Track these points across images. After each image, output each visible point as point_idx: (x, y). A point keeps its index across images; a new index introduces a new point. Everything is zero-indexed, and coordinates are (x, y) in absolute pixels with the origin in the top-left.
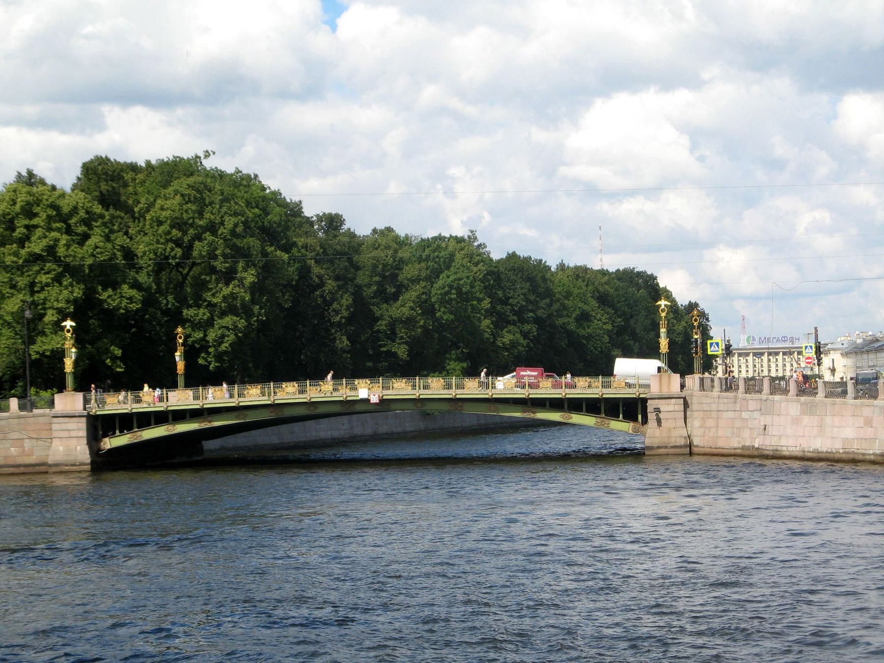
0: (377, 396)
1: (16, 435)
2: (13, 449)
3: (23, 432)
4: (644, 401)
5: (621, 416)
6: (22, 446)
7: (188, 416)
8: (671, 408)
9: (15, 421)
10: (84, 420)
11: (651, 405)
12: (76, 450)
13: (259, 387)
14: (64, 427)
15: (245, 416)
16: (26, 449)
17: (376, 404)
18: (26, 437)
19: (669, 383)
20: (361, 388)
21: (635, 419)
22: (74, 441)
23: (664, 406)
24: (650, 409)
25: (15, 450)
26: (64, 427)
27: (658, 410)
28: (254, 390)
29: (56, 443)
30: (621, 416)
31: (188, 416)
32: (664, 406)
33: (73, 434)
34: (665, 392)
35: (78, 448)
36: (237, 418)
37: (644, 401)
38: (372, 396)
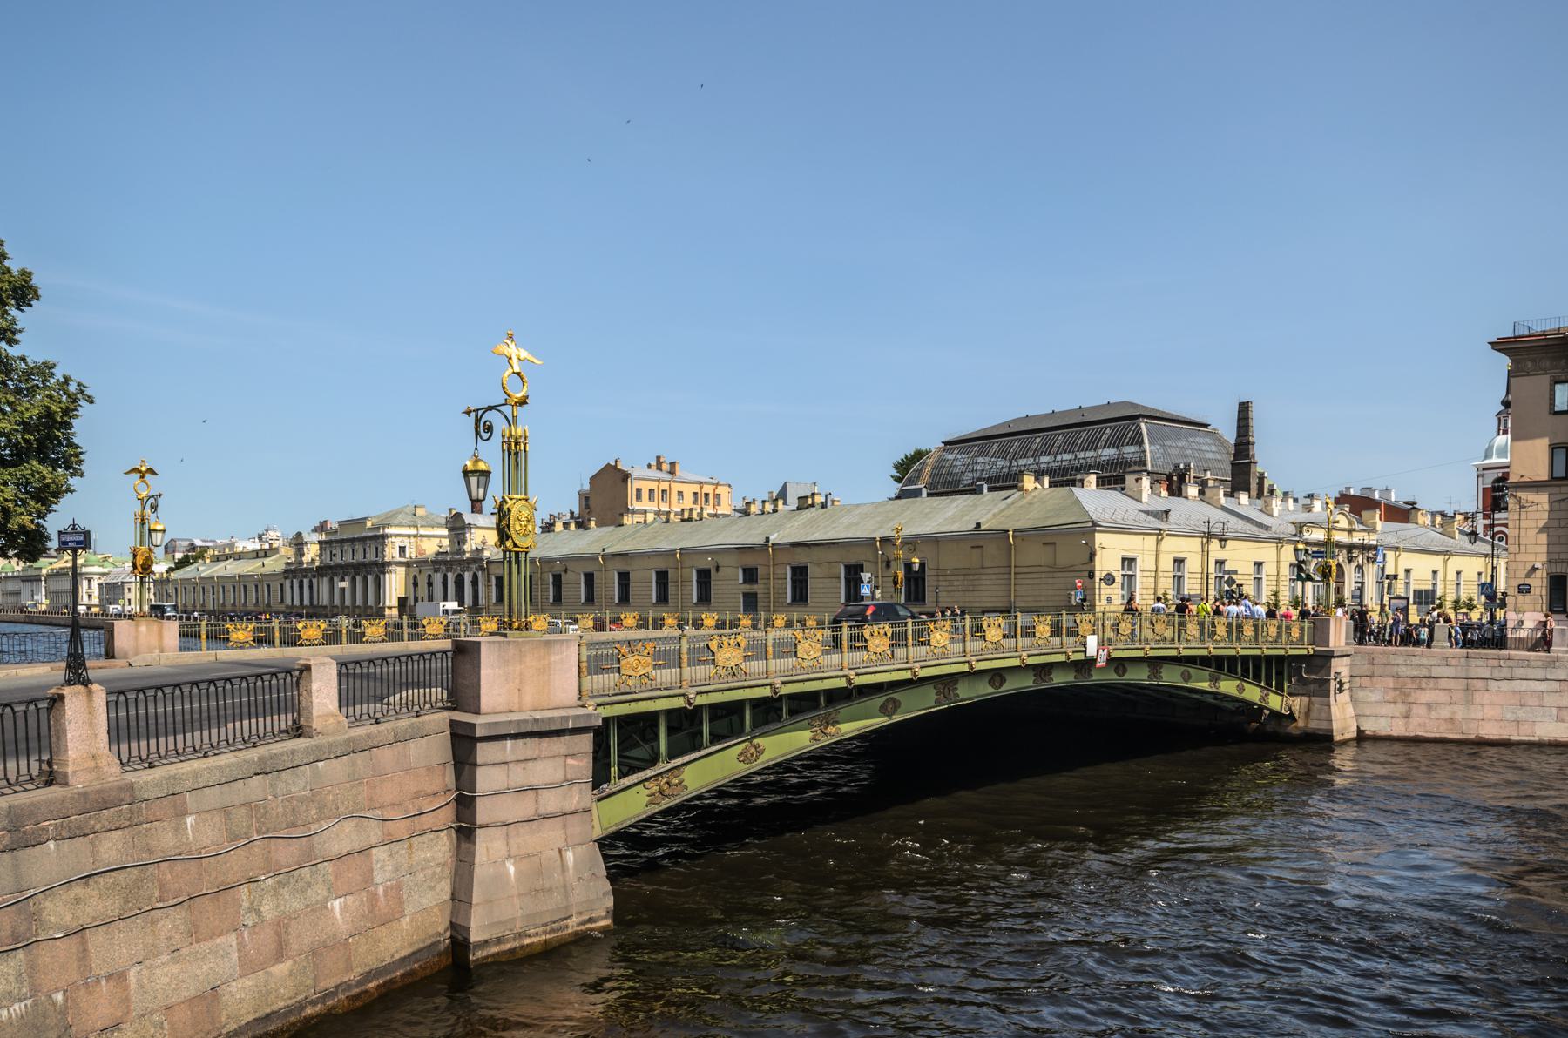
2: (336, 904)
22: (552, 834)
25: (344, 909)
26: (519, 776)
29: (487, 846)
33: (551, 802)
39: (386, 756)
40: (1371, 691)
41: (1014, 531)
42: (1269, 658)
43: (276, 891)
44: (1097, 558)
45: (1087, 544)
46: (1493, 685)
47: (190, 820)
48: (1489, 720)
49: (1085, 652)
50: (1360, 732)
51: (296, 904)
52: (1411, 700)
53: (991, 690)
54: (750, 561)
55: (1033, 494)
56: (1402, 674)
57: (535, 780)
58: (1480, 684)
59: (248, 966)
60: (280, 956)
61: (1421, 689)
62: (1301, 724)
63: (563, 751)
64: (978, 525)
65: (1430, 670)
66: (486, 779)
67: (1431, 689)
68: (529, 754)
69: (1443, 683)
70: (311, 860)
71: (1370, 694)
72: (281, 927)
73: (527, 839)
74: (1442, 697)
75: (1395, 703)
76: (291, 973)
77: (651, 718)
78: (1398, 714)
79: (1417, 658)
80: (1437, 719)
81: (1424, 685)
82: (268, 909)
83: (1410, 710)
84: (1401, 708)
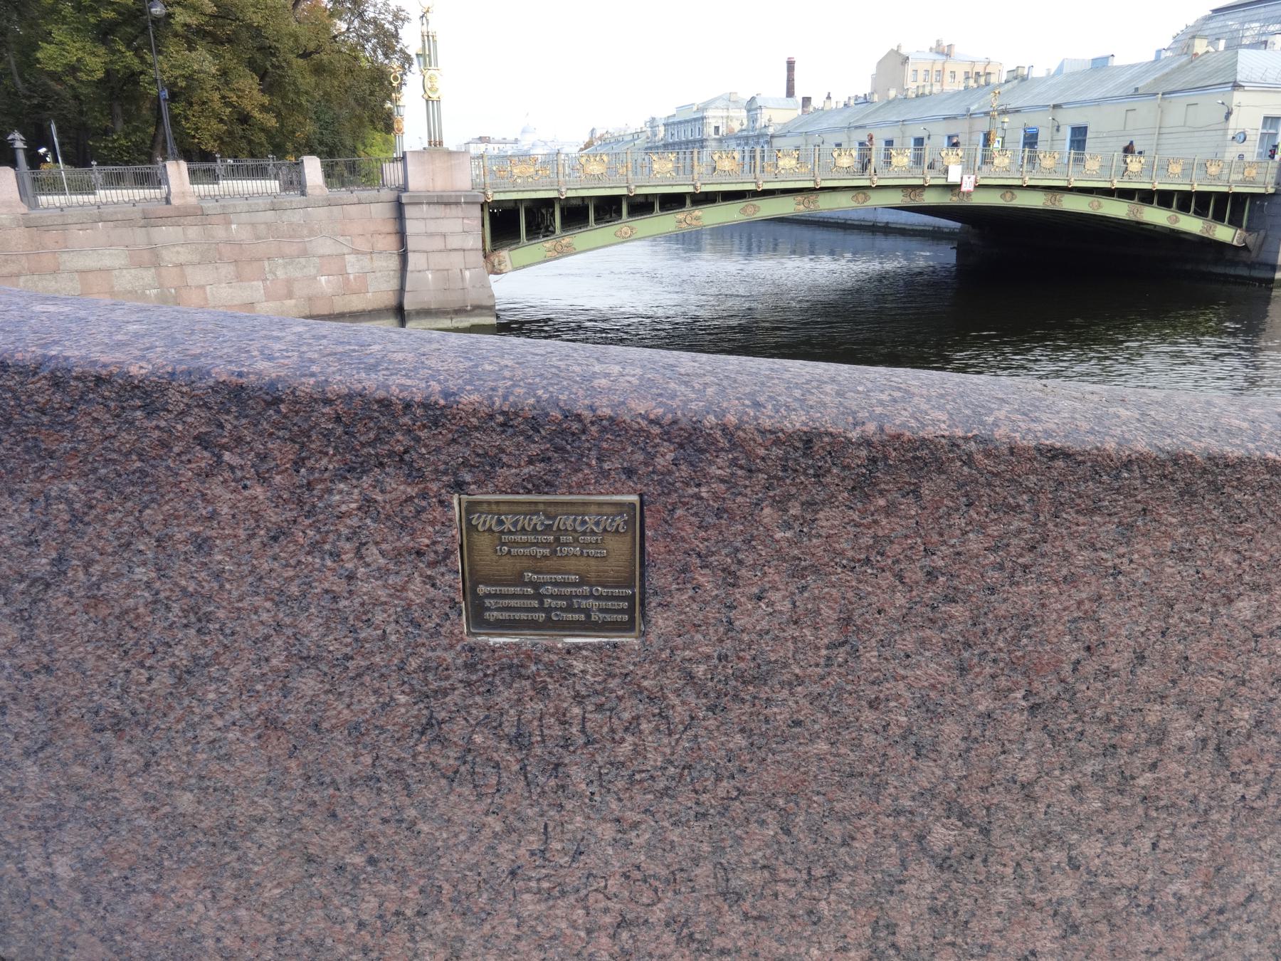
0: (973, 177)
1: (324, 246)
3: (341, 239)
6: (343, 273)
7: (657, 206)
9: (322, 212)
10: (477, 211)
12: (463, 278)
14: (433, 227)
16: (351, 277)
18: (346, 250)
22: (457, 259)
25: (327, 282)
26: (433, 227)
31: (657, 206)
33: (454, 242)
35: (467, 274)
38: (965, 177)
39: (353, 210)
42: (1236, 195)
43: (285, 267)
44: (1232, 118)
47: (234, 226)
51: (298, 274)
53: (854, 204)
54: (953, 128)
57: (443, 230)
59: (269, 297)
60: (290, 295)
62: (1254, 254)
63: (461, 214)
64: (1137, 89)
66: (411, 227)
68: (438, 215)
70: (304, 253)
72: (289, 282)
73: (441, 261)
76: (296, 306)
77: (549, 203)
82: (280, 273)
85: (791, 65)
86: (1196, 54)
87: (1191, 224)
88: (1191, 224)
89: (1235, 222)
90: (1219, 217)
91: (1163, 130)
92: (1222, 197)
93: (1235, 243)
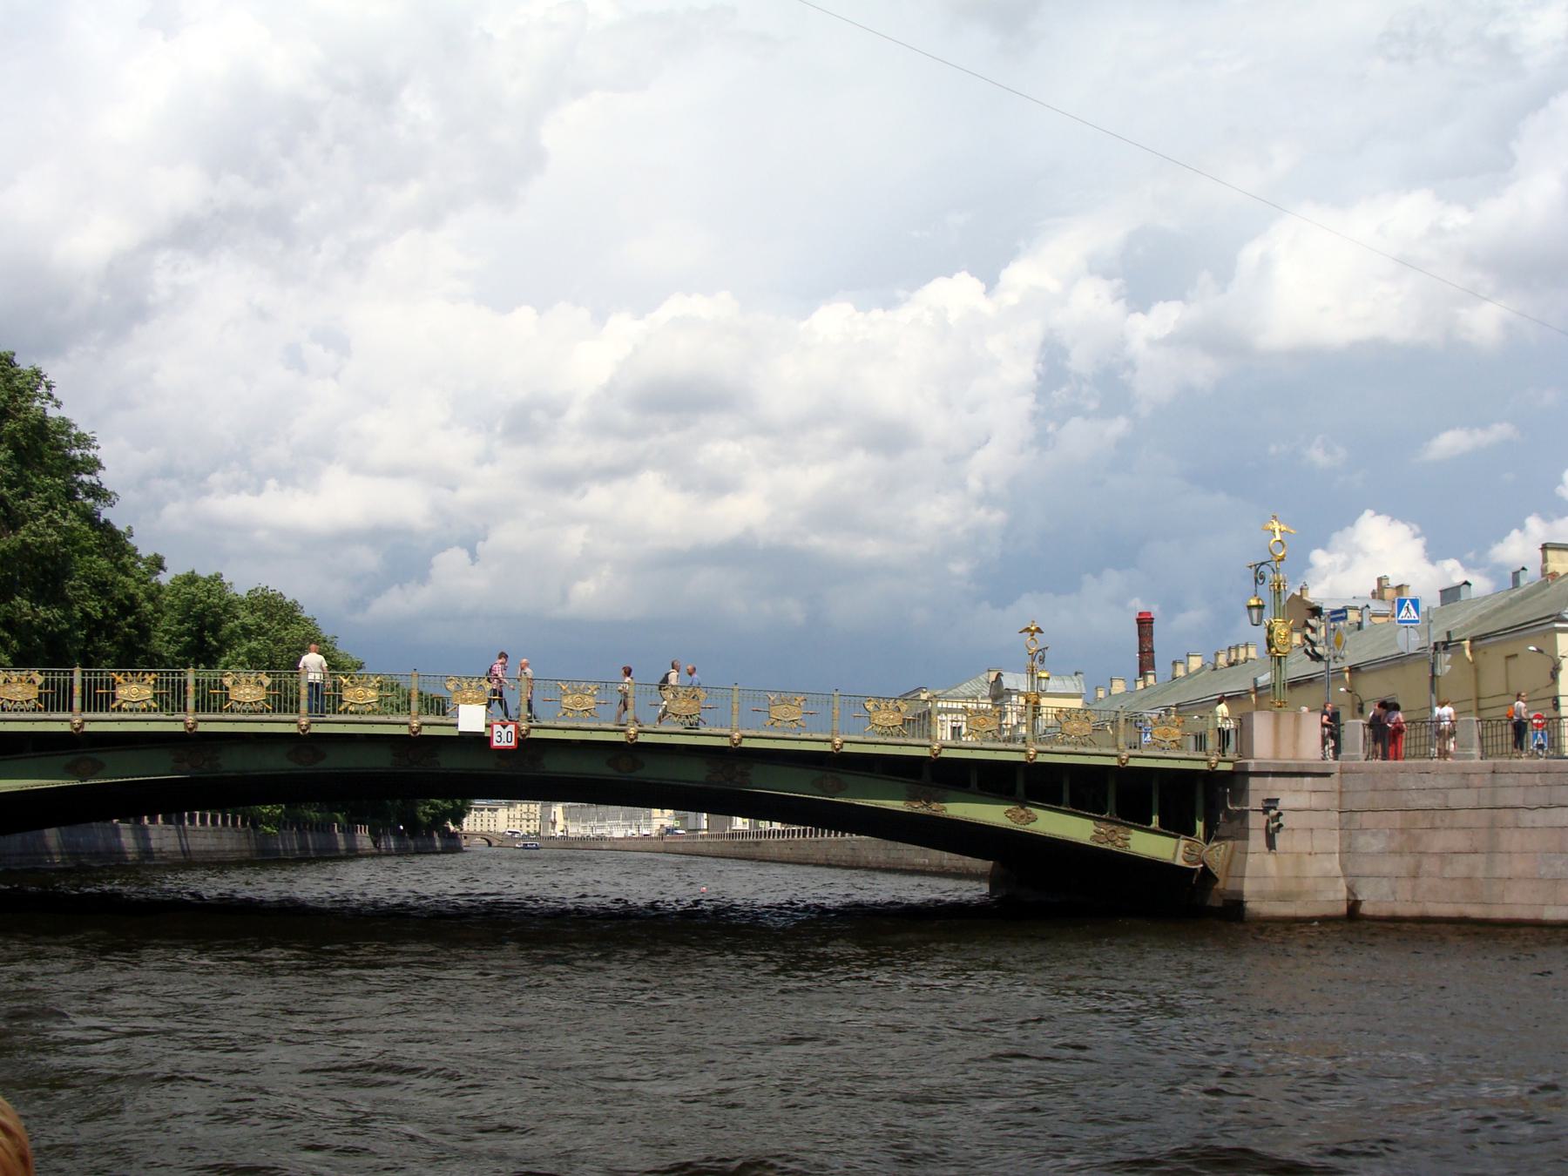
0: (511, 728)
4: (1237, 779)
5: (1155, 818)
8: (1302, 800)
11: (1258, 790)
13: (150, 679)
15: (97, 768)
17: (503, 752)
19: (1297, 736)
20: (465, 701)
21: (1189, 831)
23: (1291, 796)
24: (1255, 801)
27: (1270, 804)
28: (134, 688)
30: (1155, 818)
32: (1291, 796)
34: (1287, 758)
36: (70, 771)
37: (1237, 779)
38: (497, 728)
40: (1374, 835)
41: (1472, 640)
45: (1540, 651)
46: (1527, 818)
48: (1520, 878)
49: (456, 725)
50: (1354, 905)
52: (1421, 848)
55: (1563, 581)
56: (1412, 805)
58: (1508, 817)
61: (1433, 828)
65: (1446, 796)
67: (1446, 829)
69: (1462, 818)
71: (1373, 841)
74: (1458, 840)
75: (1400, 853)
78: (1403, 874)
79: (1432, 776)
80: (1453, 879)
81: (1438, 823)
83: (1418, 866)
84: (1409, 860)
85: (1145, 624)
86: (1554, 575)
87: (1075, 828)
88: (1075, 828)
89: (1177, 825)
90: (1138, 818)
91: (1484, 704)
92: (1124, 775)
93: (1180, 862)
